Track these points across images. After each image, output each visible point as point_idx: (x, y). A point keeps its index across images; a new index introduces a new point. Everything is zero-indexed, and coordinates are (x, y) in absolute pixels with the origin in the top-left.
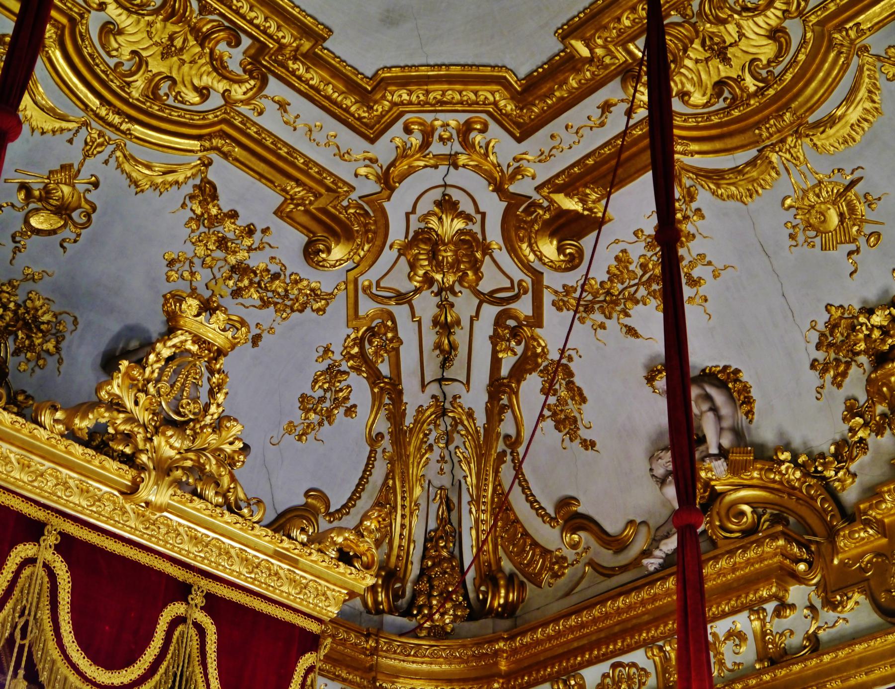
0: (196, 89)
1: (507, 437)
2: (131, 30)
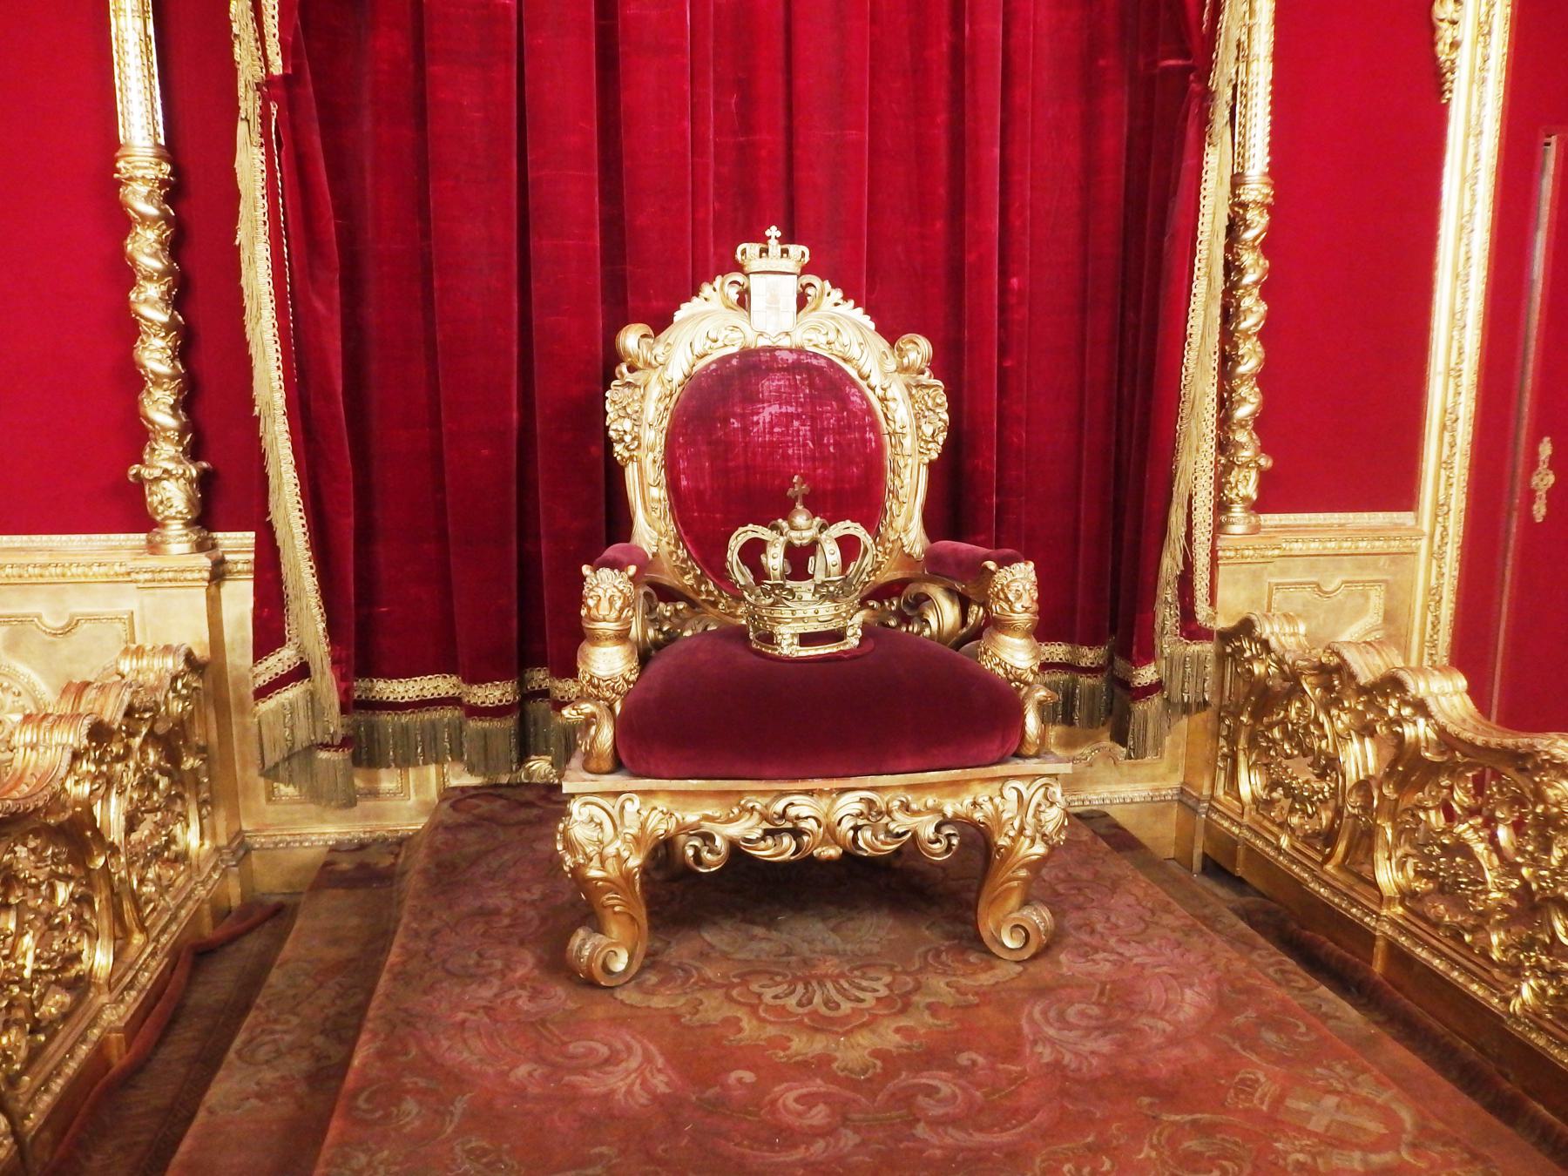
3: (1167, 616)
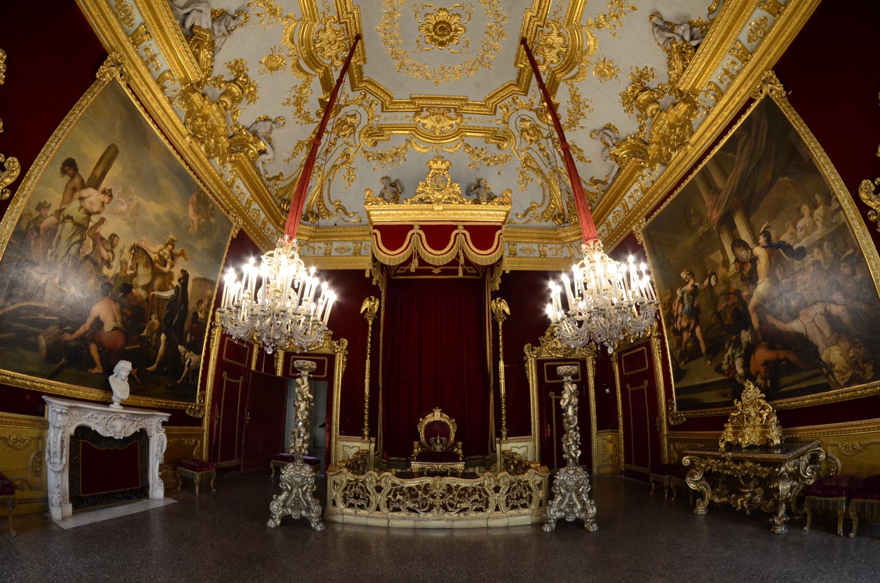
3: (490, 450)
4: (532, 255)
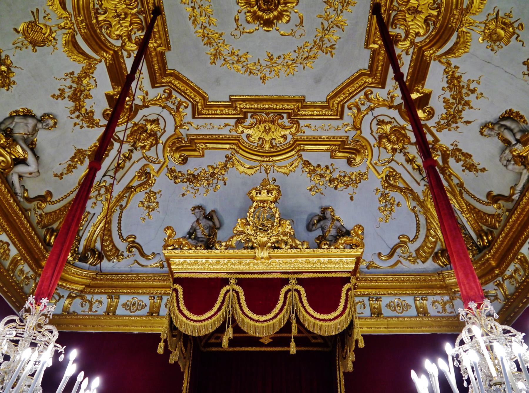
0: (282, 137)
1: (458, 184)
2: (254, 133)
4: (405, 314)
